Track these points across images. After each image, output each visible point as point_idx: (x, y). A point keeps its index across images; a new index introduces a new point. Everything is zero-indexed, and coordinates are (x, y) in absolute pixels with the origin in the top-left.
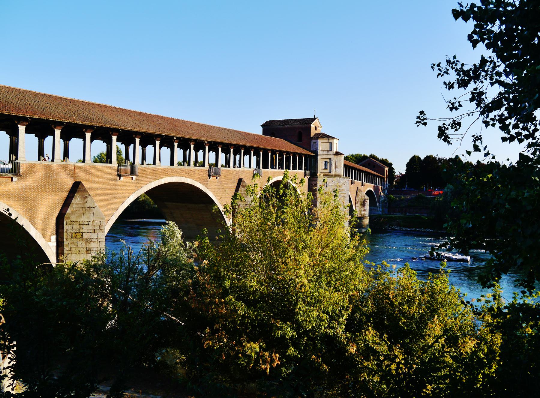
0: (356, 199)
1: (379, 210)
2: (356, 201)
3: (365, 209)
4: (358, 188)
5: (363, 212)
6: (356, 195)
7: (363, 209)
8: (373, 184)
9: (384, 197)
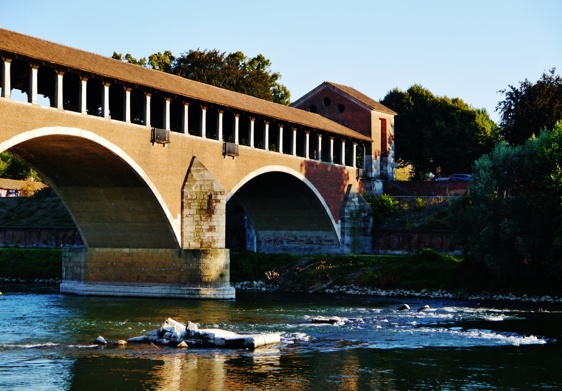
0: (182, 193)
1: (343, 242)
2: (182, 197)
3: (215, 224)
4: (194, 157)
5: (209, 234)
6: (186, 180)
7: (205, 226)
8: (300, 153)
9: (360, 201)
